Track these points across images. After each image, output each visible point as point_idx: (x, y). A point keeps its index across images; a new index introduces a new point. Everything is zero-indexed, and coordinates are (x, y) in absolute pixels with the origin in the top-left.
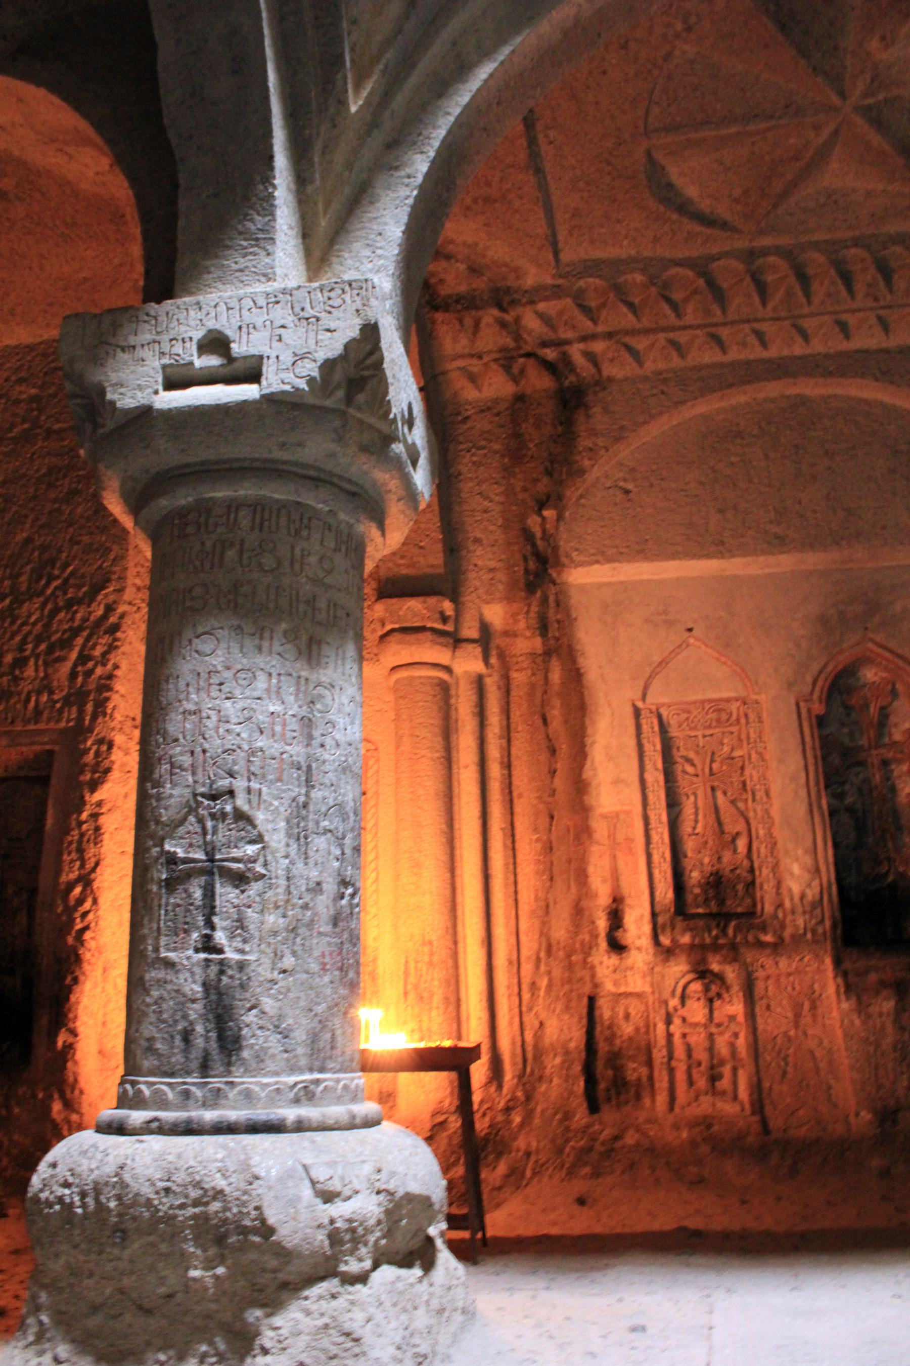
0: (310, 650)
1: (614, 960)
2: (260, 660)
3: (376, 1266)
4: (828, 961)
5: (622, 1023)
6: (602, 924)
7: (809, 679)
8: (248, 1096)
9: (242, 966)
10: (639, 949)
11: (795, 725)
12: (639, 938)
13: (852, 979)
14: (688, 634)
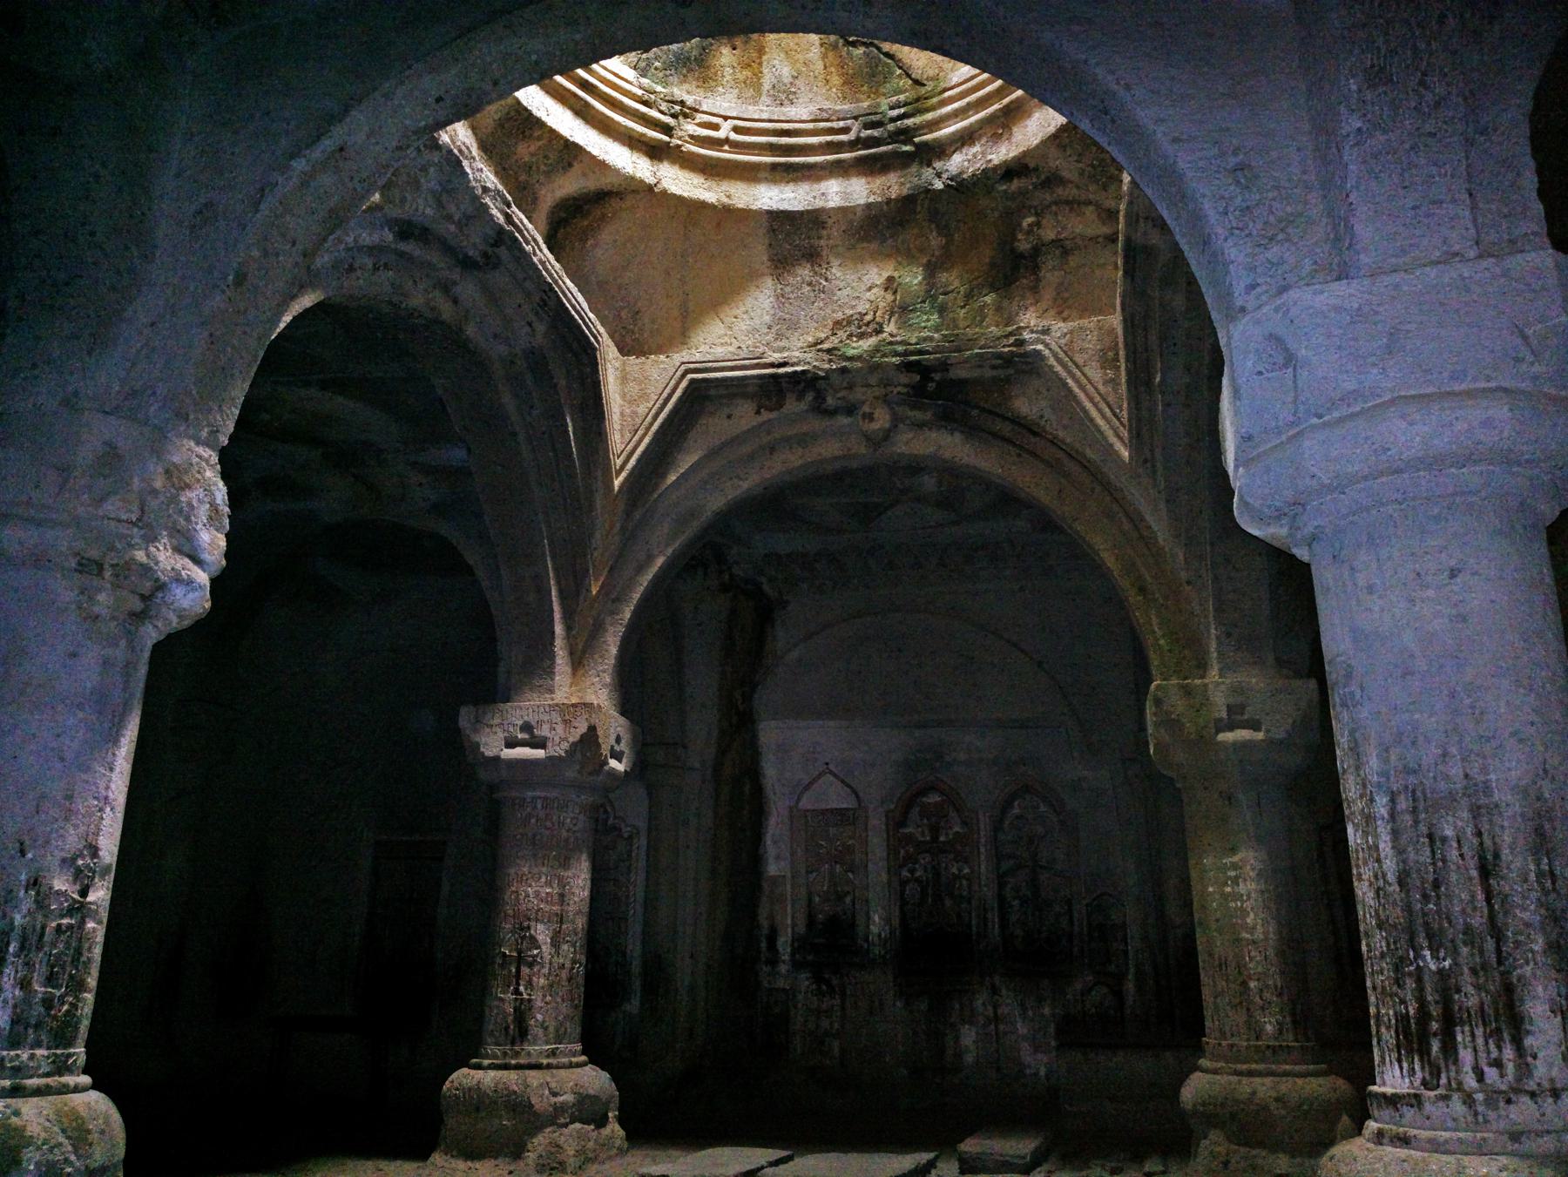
0: (565, 863)
2: (544, 869)
3: (572, 1122)
4: (890, 978)
6: (764, 945)
8: (529, 1054)
9: (530, 1001)
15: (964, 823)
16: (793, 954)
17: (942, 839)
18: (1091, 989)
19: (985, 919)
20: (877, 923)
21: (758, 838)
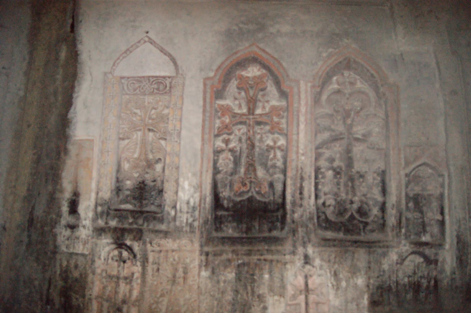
1: (68, 232)
4: (197, 246)
5: (73, 269)
6: (65, 209)
7: (215, 68)
10: (84, 227)
11: (201, 95)
12: (85, 220)
13: (211, 258)
14: (145, 34)
15: (283, 94)
16: (94, 220)
17: (259, 111)
18: (406, 257)
19: (301, 188)
20: (187, 192)
21: (68, 103)
